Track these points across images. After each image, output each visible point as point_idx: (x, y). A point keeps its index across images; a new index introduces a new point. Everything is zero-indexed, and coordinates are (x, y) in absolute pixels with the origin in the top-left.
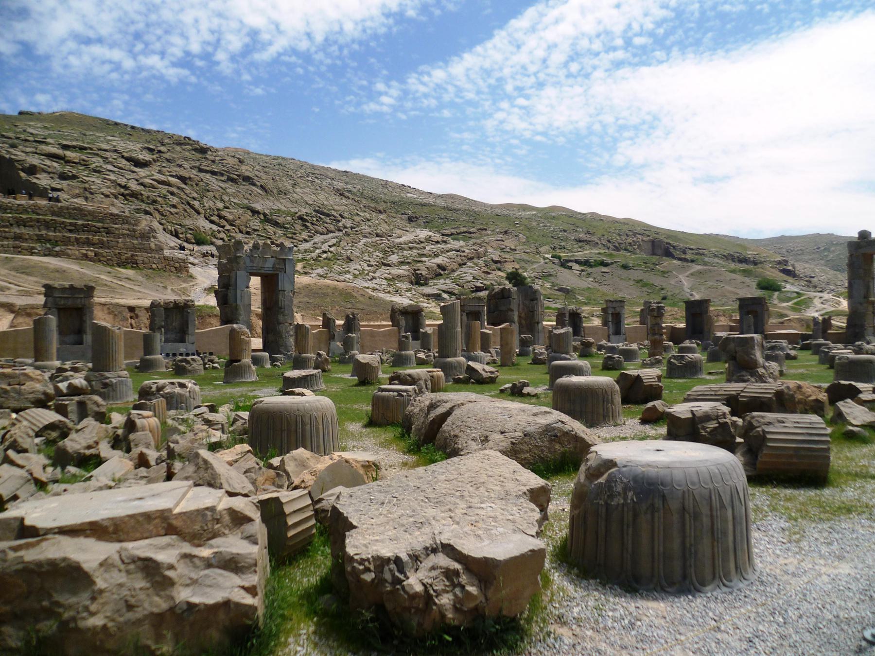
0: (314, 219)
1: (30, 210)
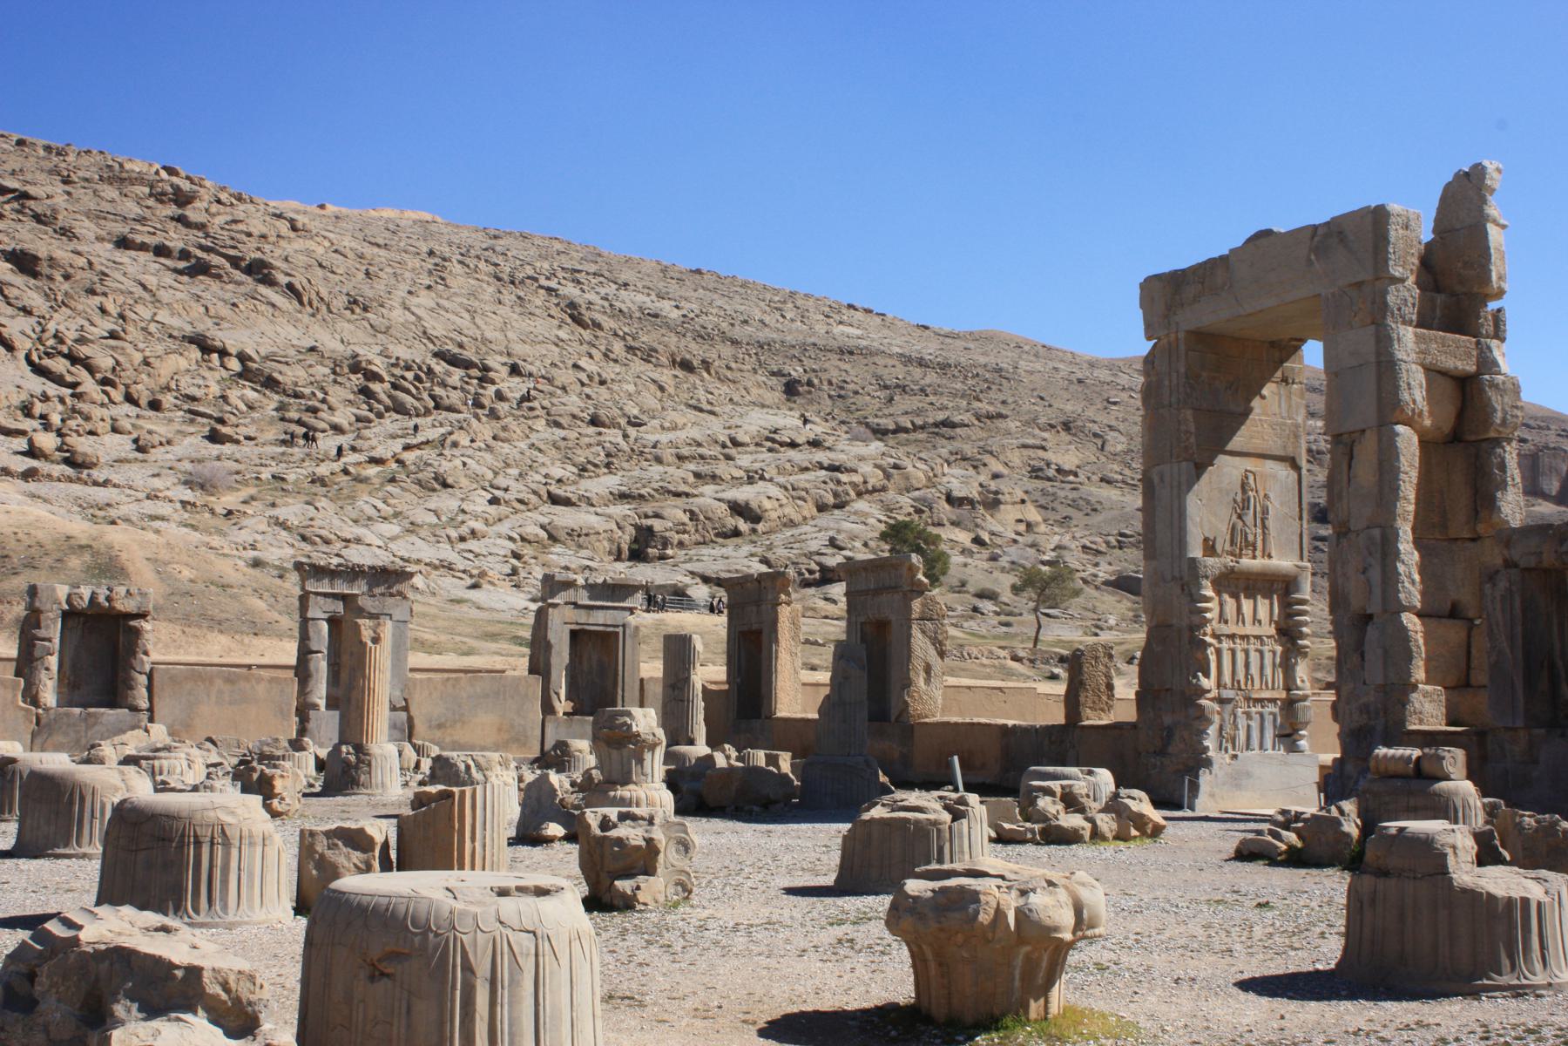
0: (410, 375)
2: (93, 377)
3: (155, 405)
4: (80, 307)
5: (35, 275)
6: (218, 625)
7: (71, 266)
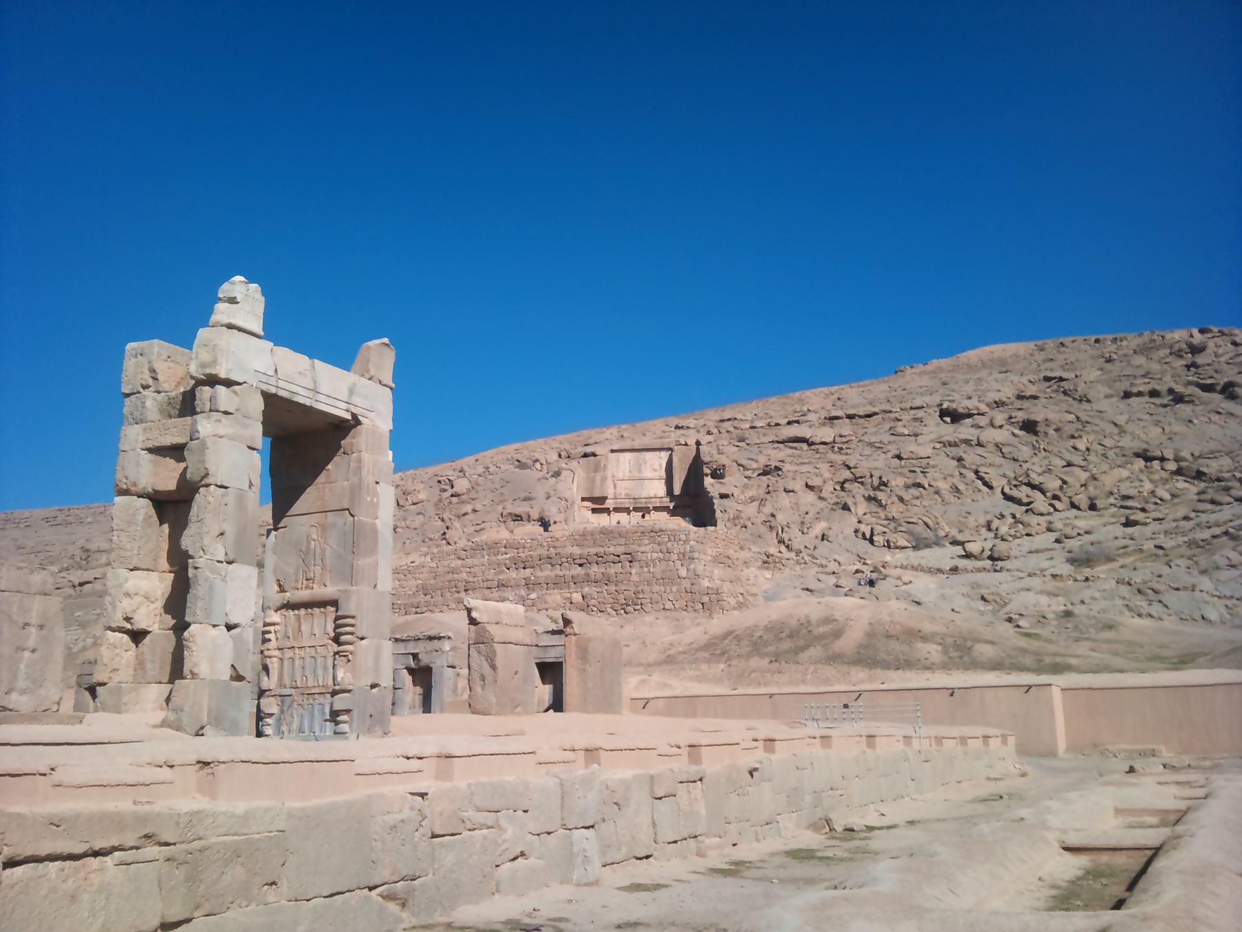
1: (545, 544)
2: (1045, 496)
3: (1093, 507)
4: (1056, 450)
5: (1036, 433)
6: (886, 666)
7: (1060, 421)
